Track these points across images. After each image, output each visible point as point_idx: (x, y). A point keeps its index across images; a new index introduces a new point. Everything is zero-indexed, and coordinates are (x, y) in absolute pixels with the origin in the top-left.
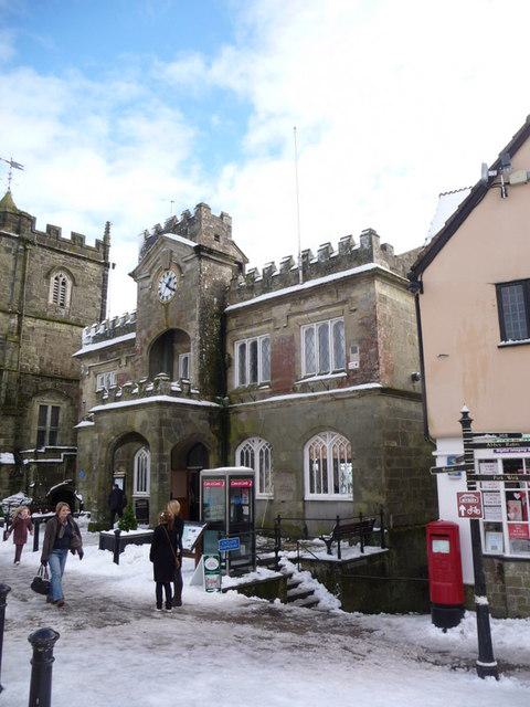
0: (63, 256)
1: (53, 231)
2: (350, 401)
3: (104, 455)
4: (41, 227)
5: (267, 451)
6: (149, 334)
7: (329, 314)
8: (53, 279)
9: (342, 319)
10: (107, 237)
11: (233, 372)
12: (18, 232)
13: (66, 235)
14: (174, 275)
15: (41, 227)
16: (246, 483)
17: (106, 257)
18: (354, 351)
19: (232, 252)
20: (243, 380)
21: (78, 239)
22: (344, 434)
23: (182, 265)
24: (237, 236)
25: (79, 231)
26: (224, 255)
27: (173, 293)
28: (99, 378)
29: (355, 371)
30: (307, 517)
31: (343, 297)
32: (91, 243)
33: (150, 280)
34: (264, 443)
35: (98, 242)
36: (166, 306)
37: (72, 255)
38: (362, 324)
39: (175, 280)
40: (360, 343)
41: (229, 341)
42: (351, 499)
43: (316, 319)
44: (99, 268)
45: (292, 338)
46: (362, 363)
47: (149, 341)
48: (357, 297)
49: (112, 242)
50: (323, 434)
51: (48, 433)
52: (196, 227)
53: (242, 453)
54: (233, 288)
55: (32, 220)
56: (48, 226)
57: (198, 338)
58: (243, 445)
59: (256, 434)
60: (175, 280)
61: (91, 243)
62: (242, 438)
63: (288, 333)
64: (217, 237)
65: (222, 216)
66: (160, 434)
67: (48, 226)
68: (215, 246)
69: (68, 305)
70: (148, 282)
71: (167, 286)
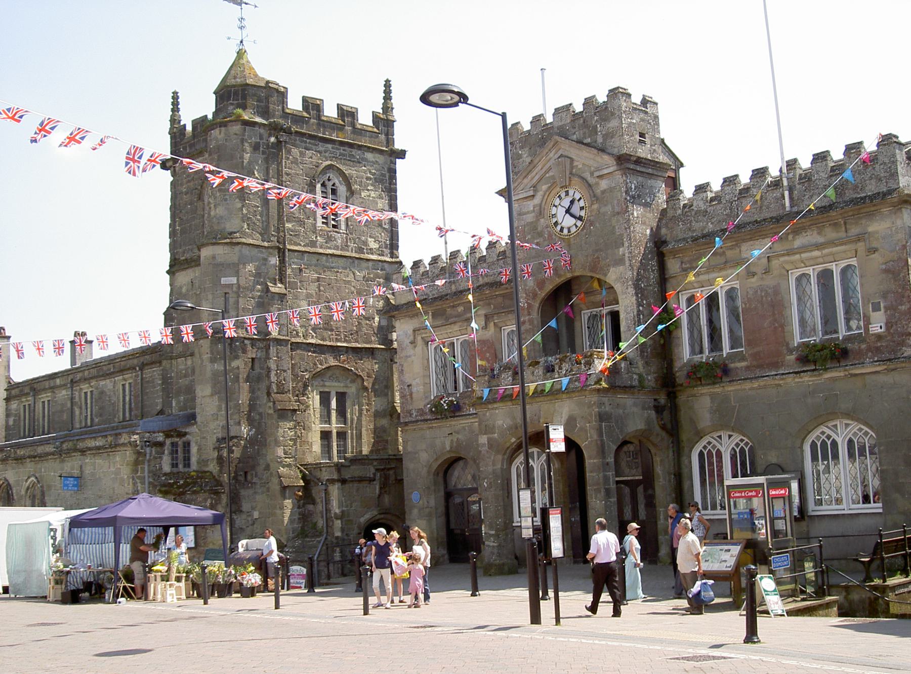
0: (330, 146)
1: (312, 106)
2: (874, 377)
3: (499, 466)
4: (294, 104)
5: (742, 451)
6: (541, 284)
7: (833, 254)
8: (319, 186)
9: (853, 262)
10: (387, 107)
11: (680, 338)
12: (265, 113)
13: (330, 112)
14: (577, 196)
15: (294, 104)
16: (783, 492)
17: (390, 141)
18: (876, 308)
19: (663, 158)
20: (697, 348)
21: (347, 114)
22: (866, 424)
23: (591, 180)
24: (667, 132)
25: (349, 102)
26: (655, 164)
27: (579, 223)
28: (432, 347)
29: (879, 337)
30: (812, 535)
31: (854, 231)
32: (365, 119)
33: (537, 201)
34: (737, 438)
35: (375, 116)
36: (567, 242)
37: (342, 143)
38: (887, 271)
39: (582, 203)
40: (884, 296)
41: (671, 293)
42: (881, 511)
43: (814, 262)
44: (380, 159)
45: (776, 291)
46: (889, 325)
47: (542, 294)
48: (877, 232)
49: (396, 114)
50: (830, 424)
51: (334, 431)
52: (613, 124)
53: (701, 454)
54: (670, 213)
55: (282, 95)
56: (305, 100)
57: (631, 291)
58: (703, 442)
59: (724, 426)
60: (582, 203)
61: (365, 119)
62: (700, 435)
63: (769, 281)
64: (642, 135)
65: (645, 102)
66: (600, 434)
67: (305, 100)
68: (643, 152)
69: (343, 227)
70: (530, 205)
71: (568, 211)
